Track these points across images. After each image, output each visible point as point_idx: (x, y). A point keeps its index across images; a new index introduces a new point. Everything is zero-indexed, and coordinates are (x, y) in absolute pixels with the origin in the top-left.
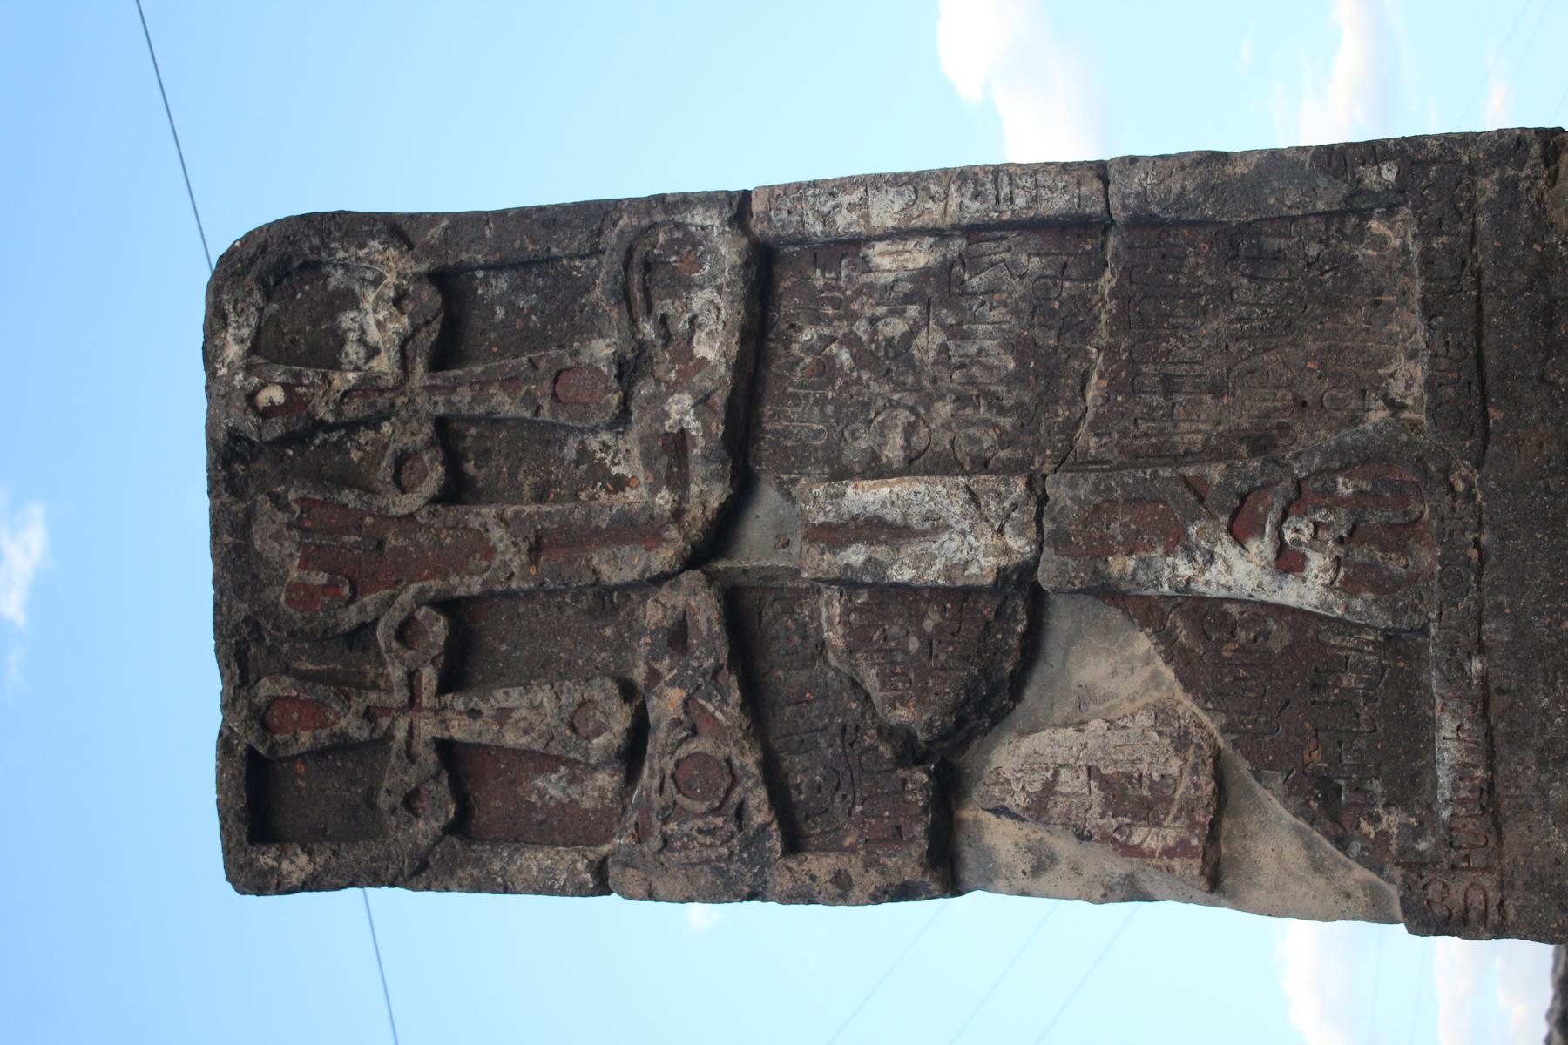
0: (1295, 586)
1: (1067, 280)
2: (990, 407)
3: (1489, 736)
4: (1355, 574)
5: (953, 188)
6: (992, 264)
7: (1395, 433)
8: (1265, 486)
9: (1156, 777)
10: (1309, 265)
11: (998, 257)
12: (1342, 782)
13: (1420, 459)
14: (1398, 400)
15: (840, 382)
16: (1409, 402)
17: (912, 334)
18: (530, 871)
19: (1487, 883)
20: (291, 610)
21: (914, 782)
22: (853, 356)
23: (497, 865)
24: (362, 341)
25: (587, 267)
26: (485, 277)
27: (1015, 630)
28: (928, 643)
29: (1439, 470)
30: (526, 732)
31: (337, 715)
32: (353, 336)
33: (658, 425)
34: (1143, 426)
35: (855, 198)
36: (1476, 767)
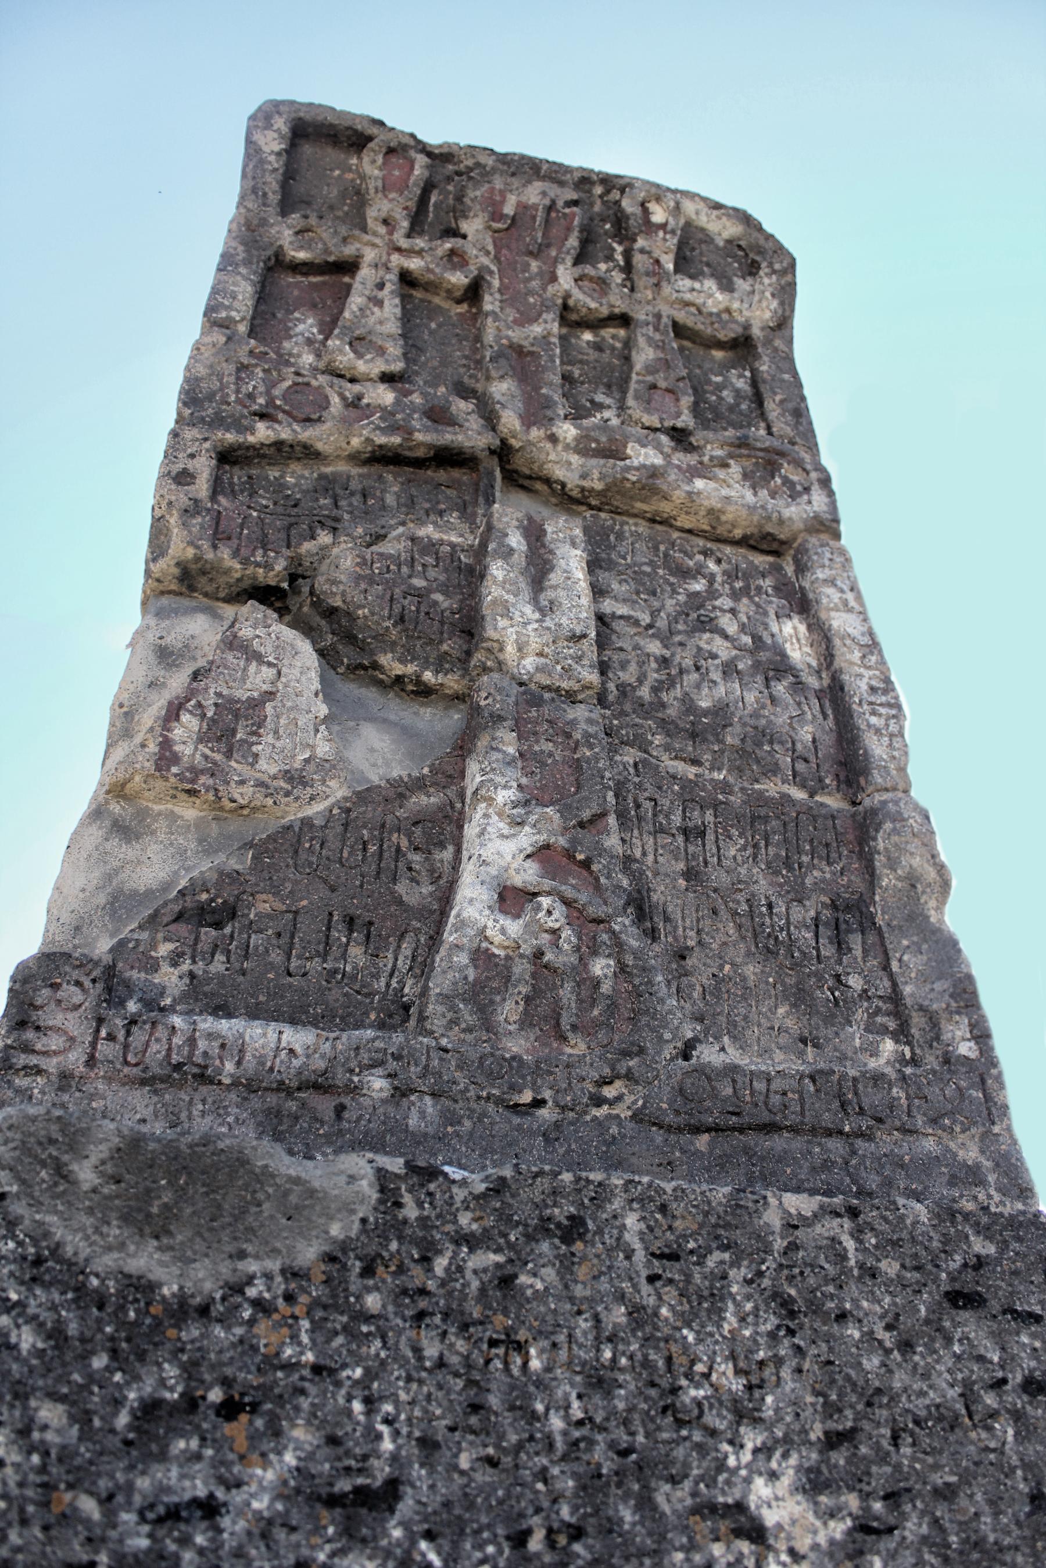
0: (485, 897)
3: (281, 1087)
4: (497, 965)
7: (671, 1026)
8: (597, 887)
9: (254, 749)
11: (806, 708)
12: (228, 930)
13: (642, 1051)
19: (72, 1056)
21: (276, 558)
22: (698, 593)
27: (427, 669)
28: (420, 595)
29: (629, 1069)
35: (852, 603)
36: (239, 1063)
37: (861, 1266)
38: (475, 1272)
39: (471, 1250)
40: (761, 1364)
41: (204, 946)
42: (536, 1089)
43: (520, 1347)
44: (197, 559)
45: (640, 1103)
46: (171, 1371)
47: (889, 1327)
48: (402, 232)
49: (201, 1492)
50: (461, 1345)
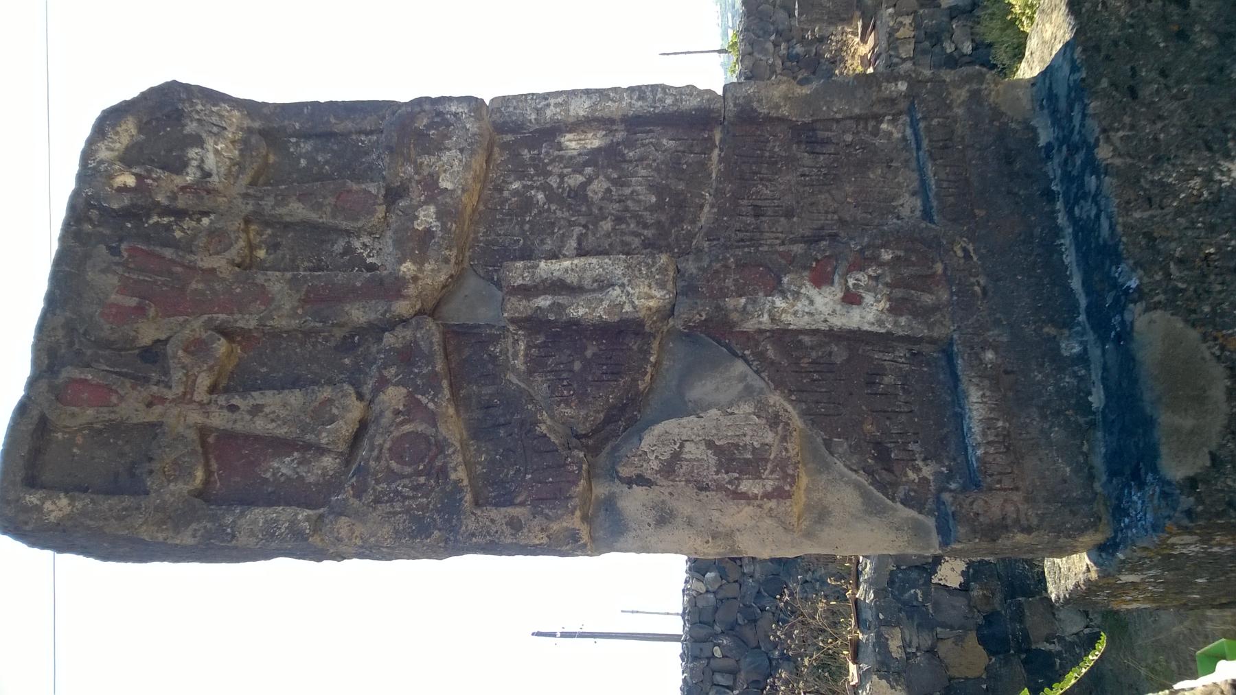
1: (692, 153)
2: (638, 224)
6: (643, 145)
10: (847, 146)
13: (935, 237)
15: (536, 211)
17: (584, 186)
19: (1016, 498)
20: (102, 321)
21: (572, 457)
24: (200, 167)
25: (369, 141)
26: (297, 142)
27: (649, 360)
30: (273, 421)
31: (122, 398)
33: (409, 224)
34: (740, 235)
35: (560, 100)
41: (902, 455)
42: (973, 285)
45: (965, 239)
50: (1212, 277)
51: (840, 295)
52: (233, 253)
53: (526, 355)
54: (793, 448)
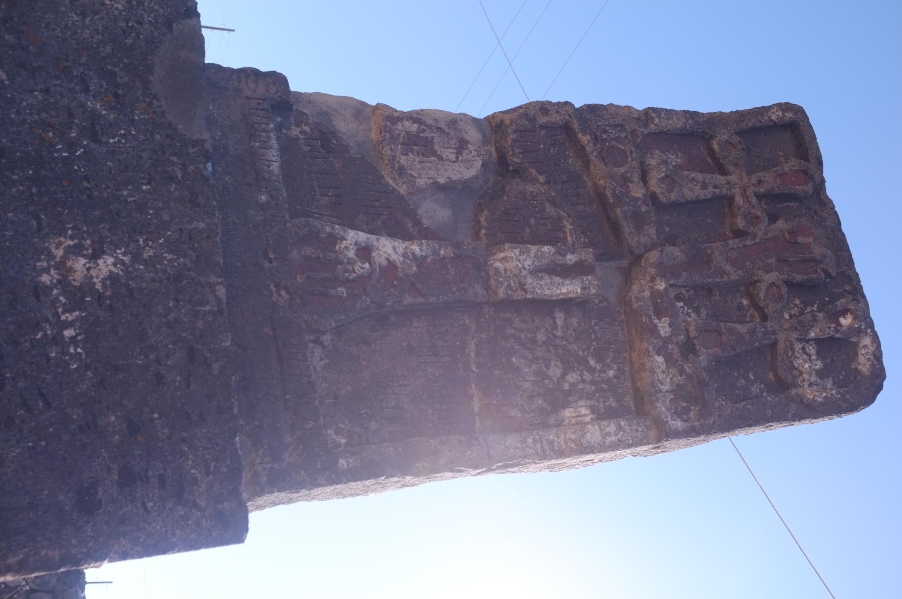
0: (361, 239)
2: (520, 337)
5: (564, 446)
14: (317, 345)
15: (592, 350)
16: (311, 345)
17: (564, 375)
18: (676, 118)
19: (248, 92)
21: (520, 158)
22: (588, 363)
23: (690, 122)
25: (719, 401)
26: (762, 393)
27: (486, 230)
30: (693, 178)
32: (814, 357)
35: (609, 440)
36: (259, 147)
37: (199, 311)
38: (173, 170)
39: (181, 169)
40: (155, 267)
43: (148, 183)
44: (506, 127)
45: (280, 304)
46: (126, 79)
47: (175, 319)
48: (756, 190)
49: (91, 88)
50: (147, 165)
51: (374, 254)
52: (763, 286)
53: (565, 233)
54: (387, 151)
